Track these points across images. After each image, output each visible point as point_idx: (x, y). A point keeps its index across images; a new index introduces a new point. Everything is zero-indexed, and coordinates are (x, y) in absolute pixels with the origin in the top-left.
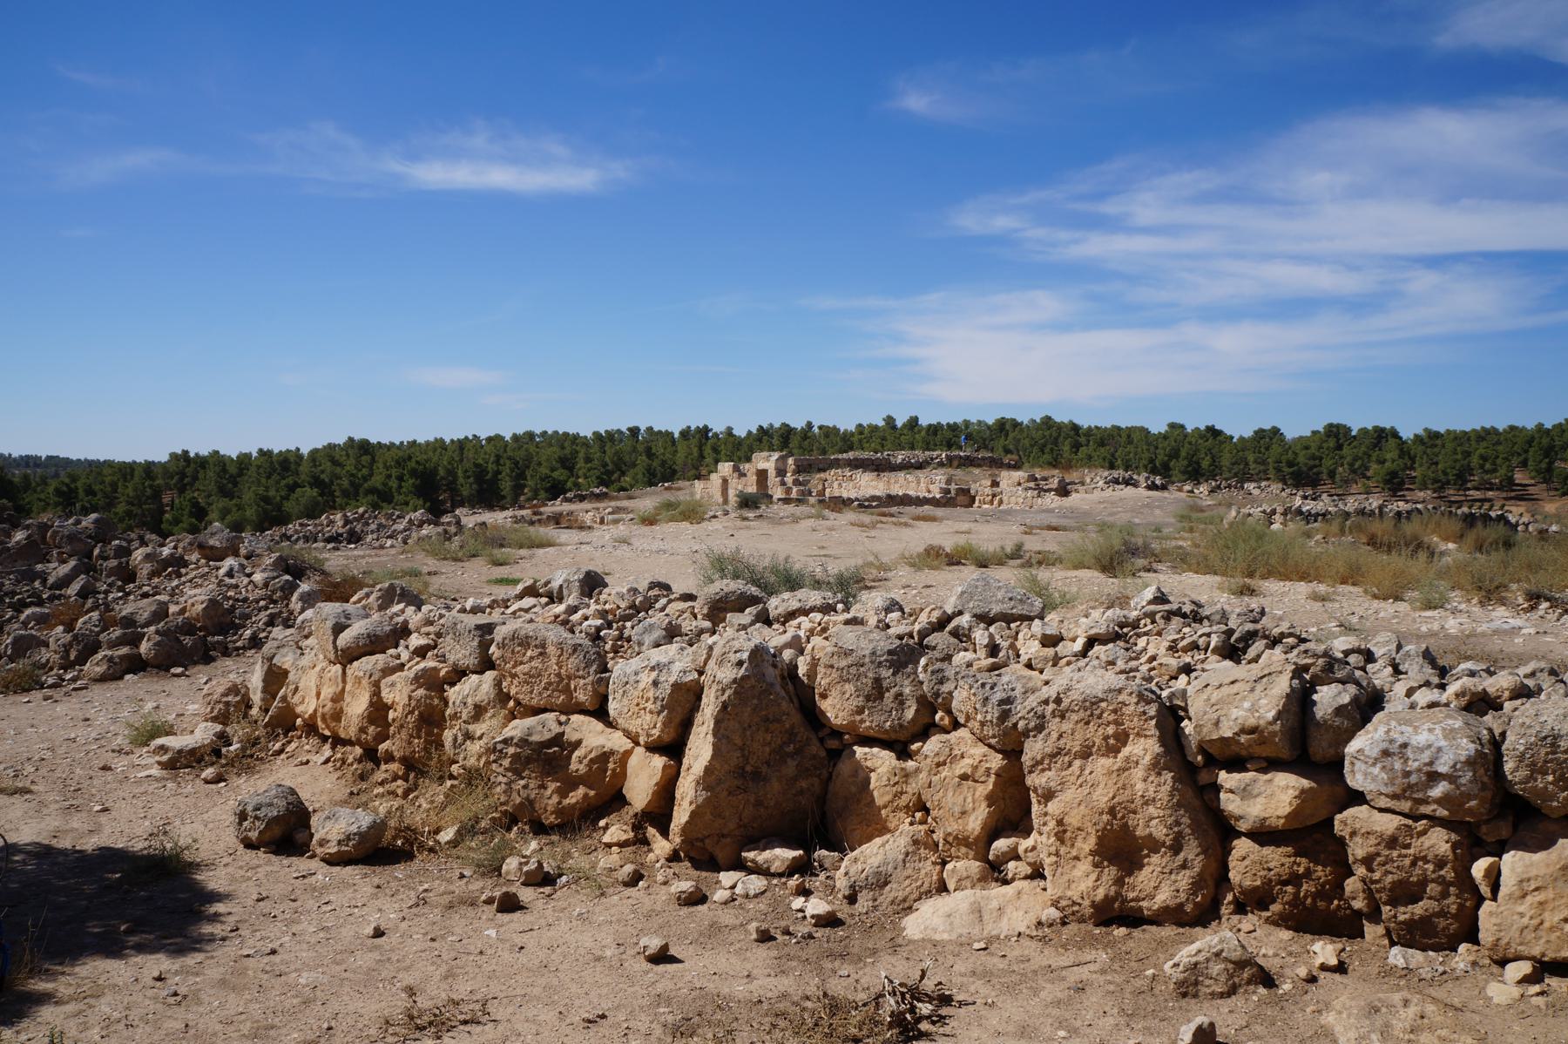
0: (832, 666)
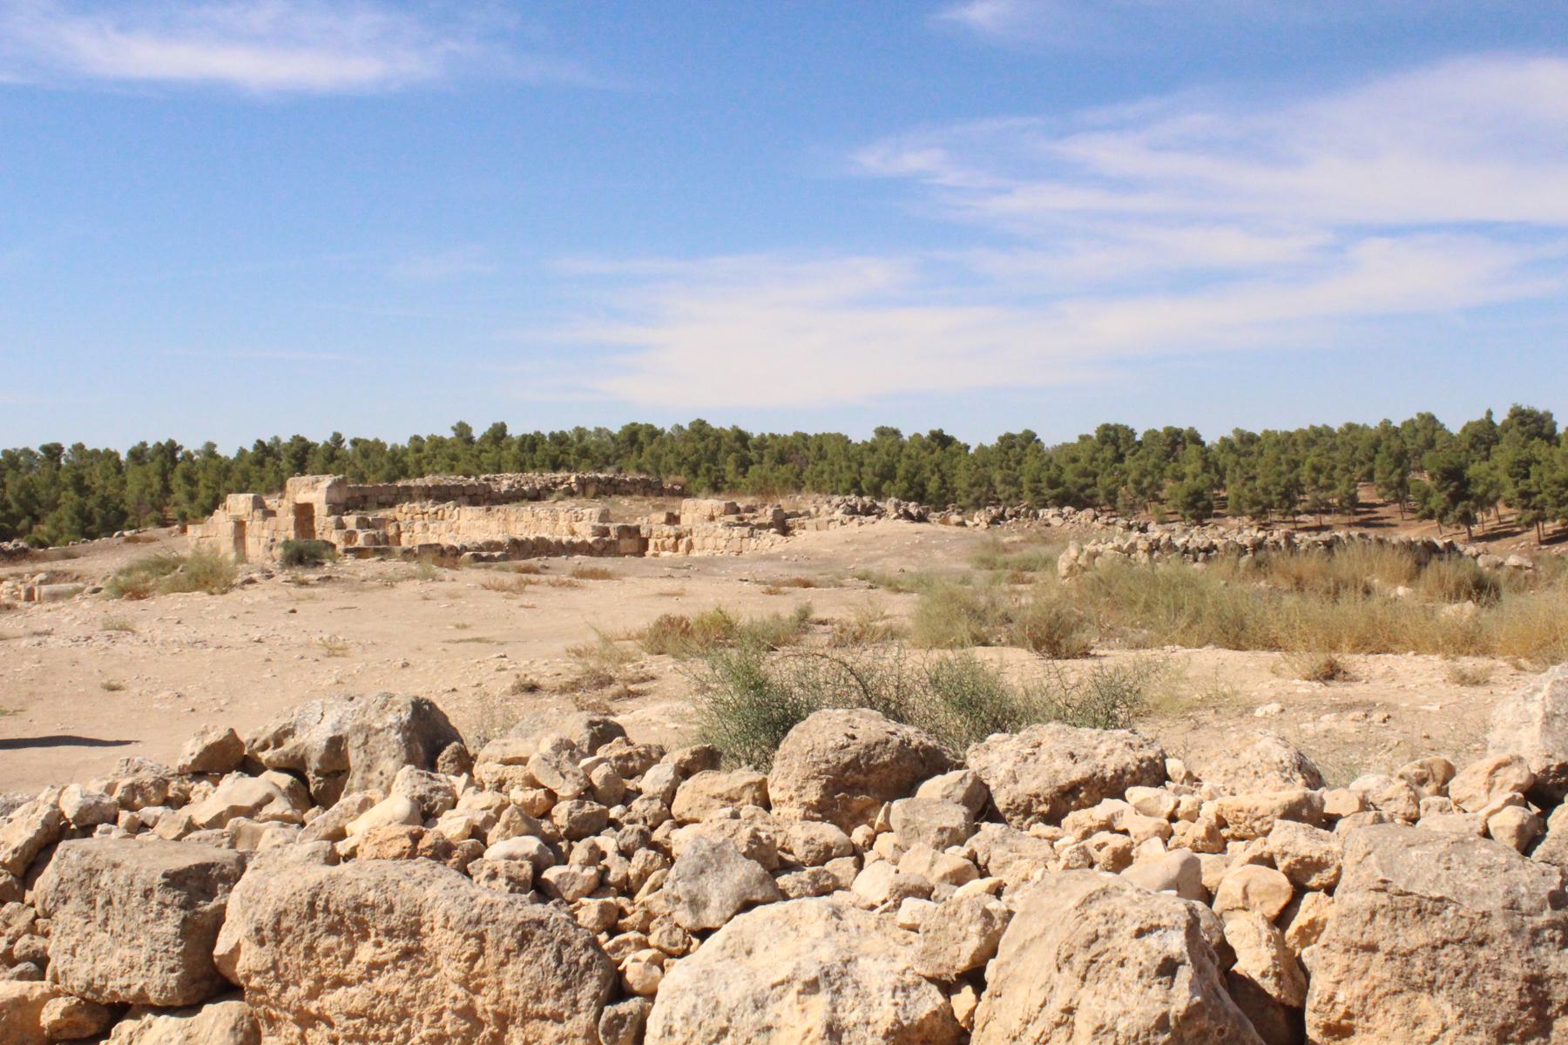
0: (1372, 948)
